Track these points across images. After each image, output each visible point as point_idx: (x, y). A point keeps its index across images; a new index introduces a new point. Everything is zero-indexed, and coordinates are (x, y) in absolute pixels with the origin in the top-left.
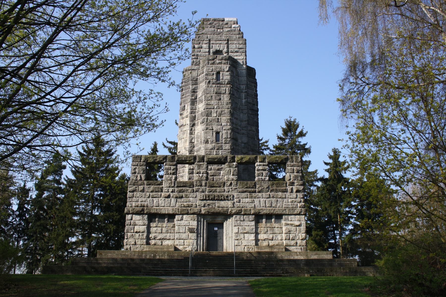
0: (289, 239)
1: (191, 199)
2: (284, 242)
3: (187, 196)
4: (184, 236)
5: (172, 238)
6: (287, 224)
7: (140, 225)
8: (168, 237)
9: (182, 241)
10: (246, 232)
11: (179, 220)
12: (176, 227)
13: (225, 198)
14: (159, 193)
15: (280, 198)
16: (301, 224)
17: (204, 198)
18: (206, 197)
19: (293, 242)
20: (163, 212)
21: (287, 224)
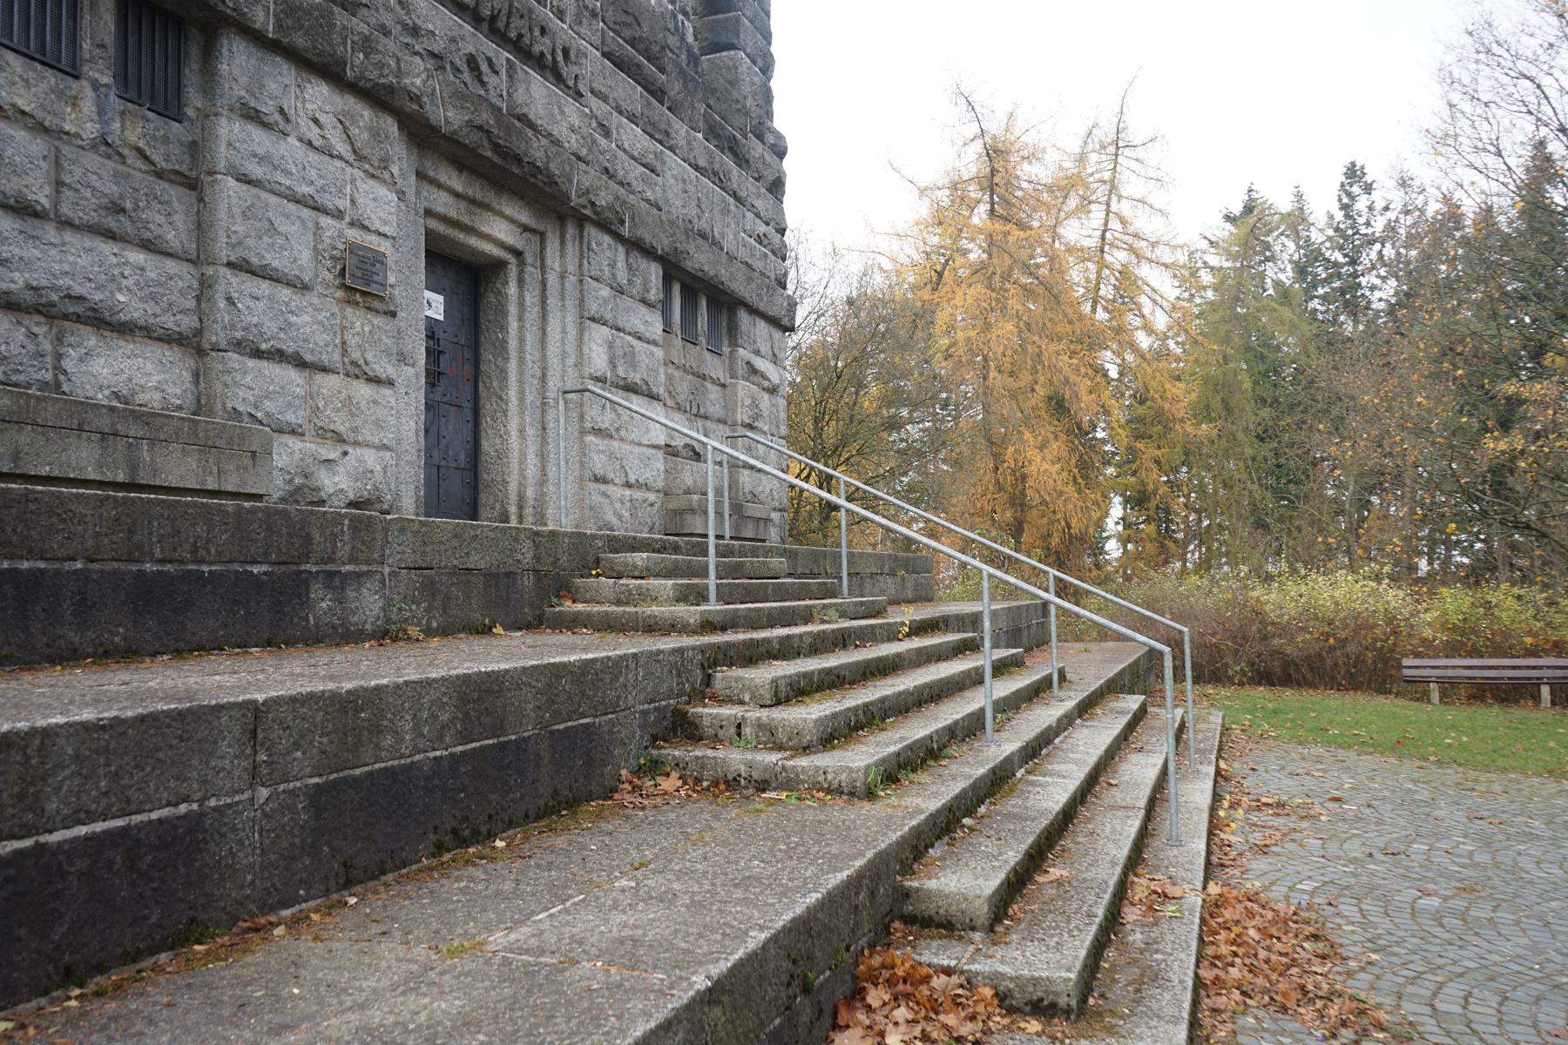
5: (169, 321)
8: (128, 304)
9: (292, 374)
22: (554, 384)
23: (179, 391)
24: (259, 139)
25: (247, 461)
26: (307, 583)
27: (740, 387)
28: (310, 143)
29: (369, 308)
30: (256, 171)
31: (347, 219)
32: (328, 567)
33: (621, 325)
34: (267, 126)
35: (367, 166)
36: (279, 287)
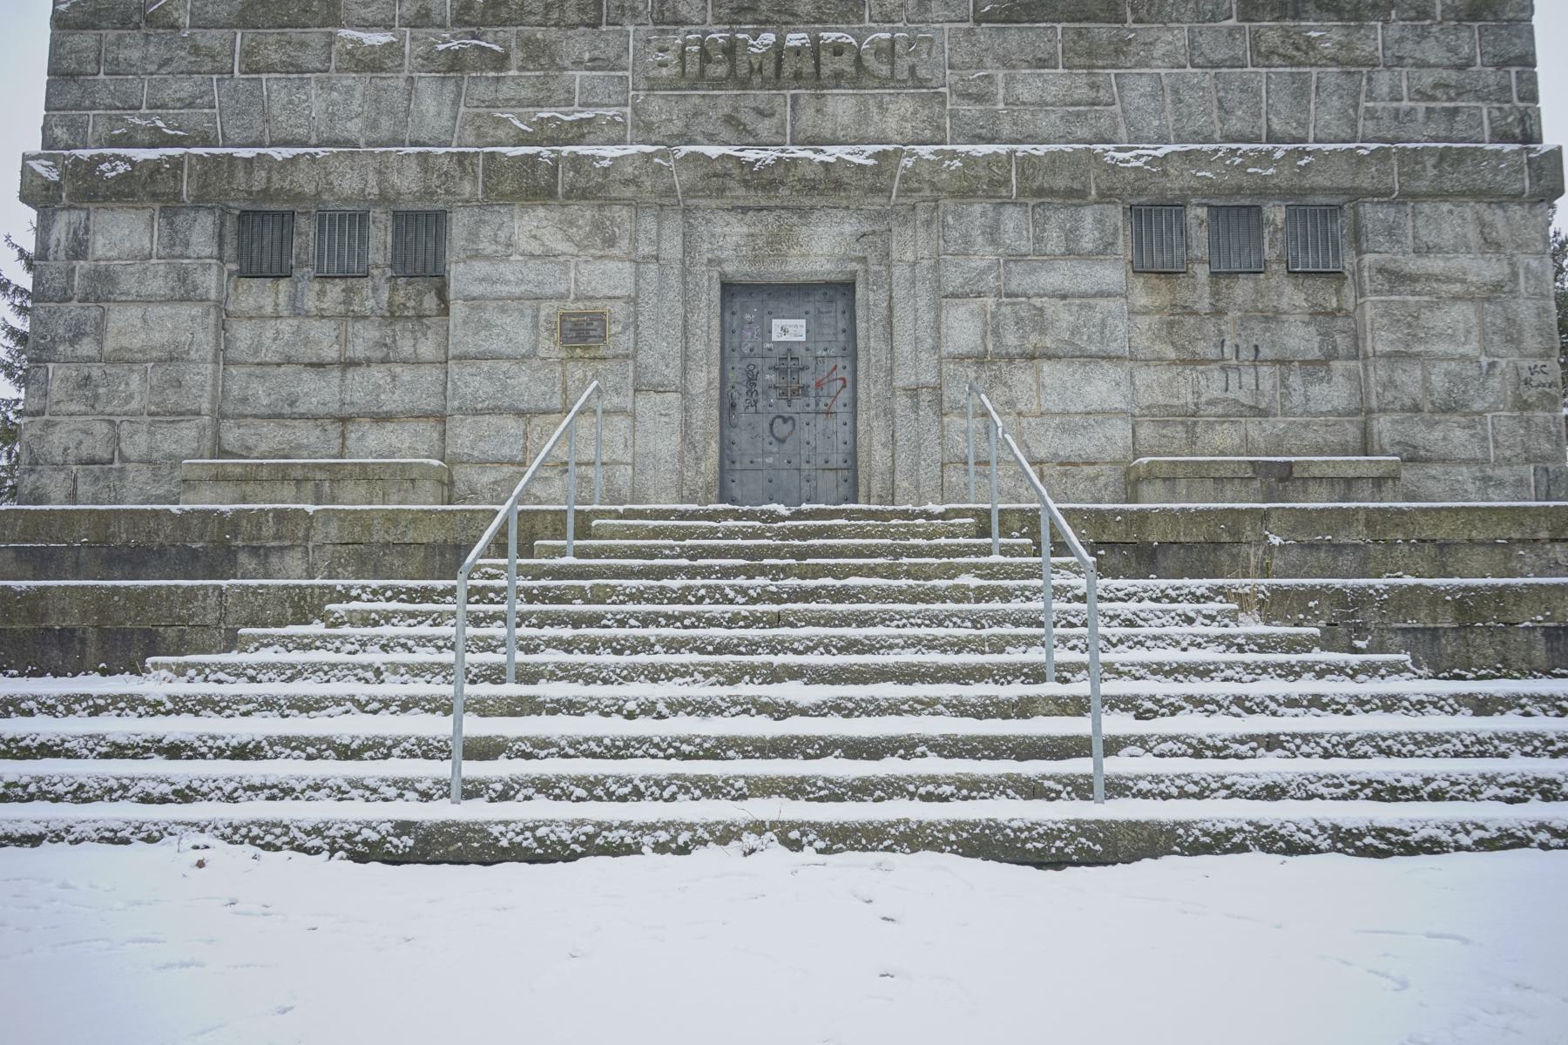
0: (1416, 409)
1: (578, 74)
2: (1383, 426)
3: (537, 53)
4: (526, 385)
6: (1396, 278)
7: (148, 300)
8: (391, 401)
10: (1048, 343)
11: (477, 255)
12: (458, 309)
13: (870, 61)
14: (315, 36)
15: (1335, 61)
16: (1515, 276)
17: (693, 68)
18: (705, 56)
19: (1454, 436)
20: (349, 183)
21: (1396, 278)
22: (904, 378)
23: (426, 447)
24: (480, 268)
25: (407, 485)
26: (235, 553)
27: (1368, 306)
28: (532, 255)
29: (594, 358)
30: (477, 290)
31: (572, 296)
32: (255, 544)
33: (1014, 286)
34: (487, 258)
35: (592, 251)
36: (501, 362)
